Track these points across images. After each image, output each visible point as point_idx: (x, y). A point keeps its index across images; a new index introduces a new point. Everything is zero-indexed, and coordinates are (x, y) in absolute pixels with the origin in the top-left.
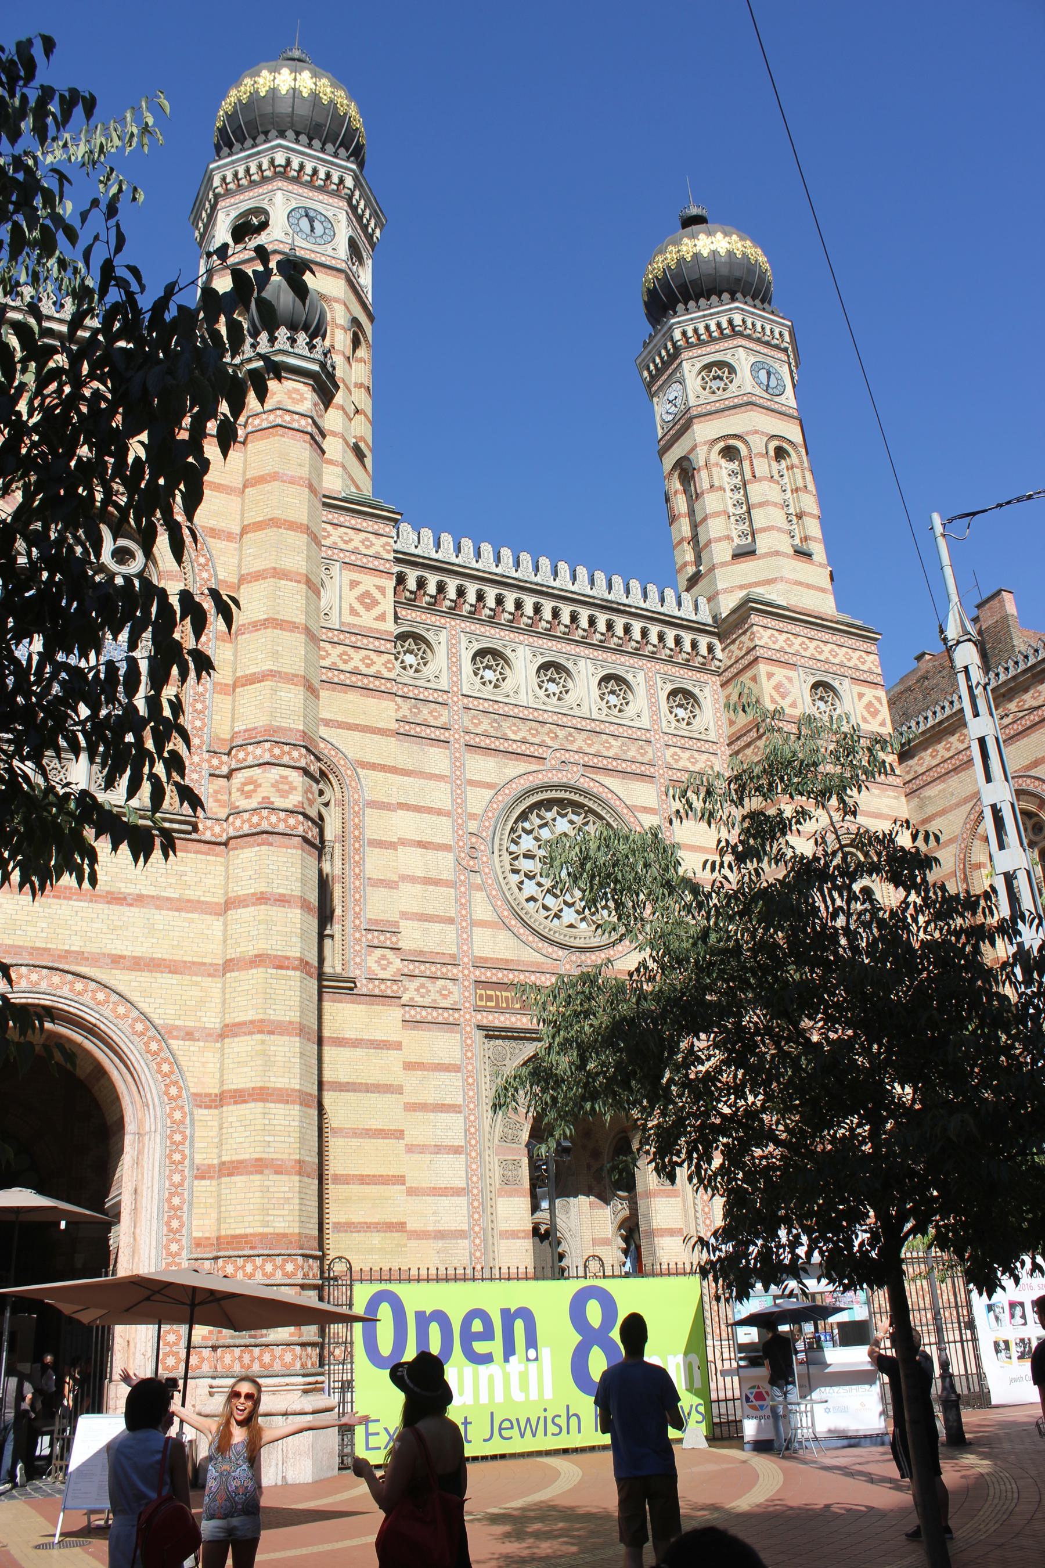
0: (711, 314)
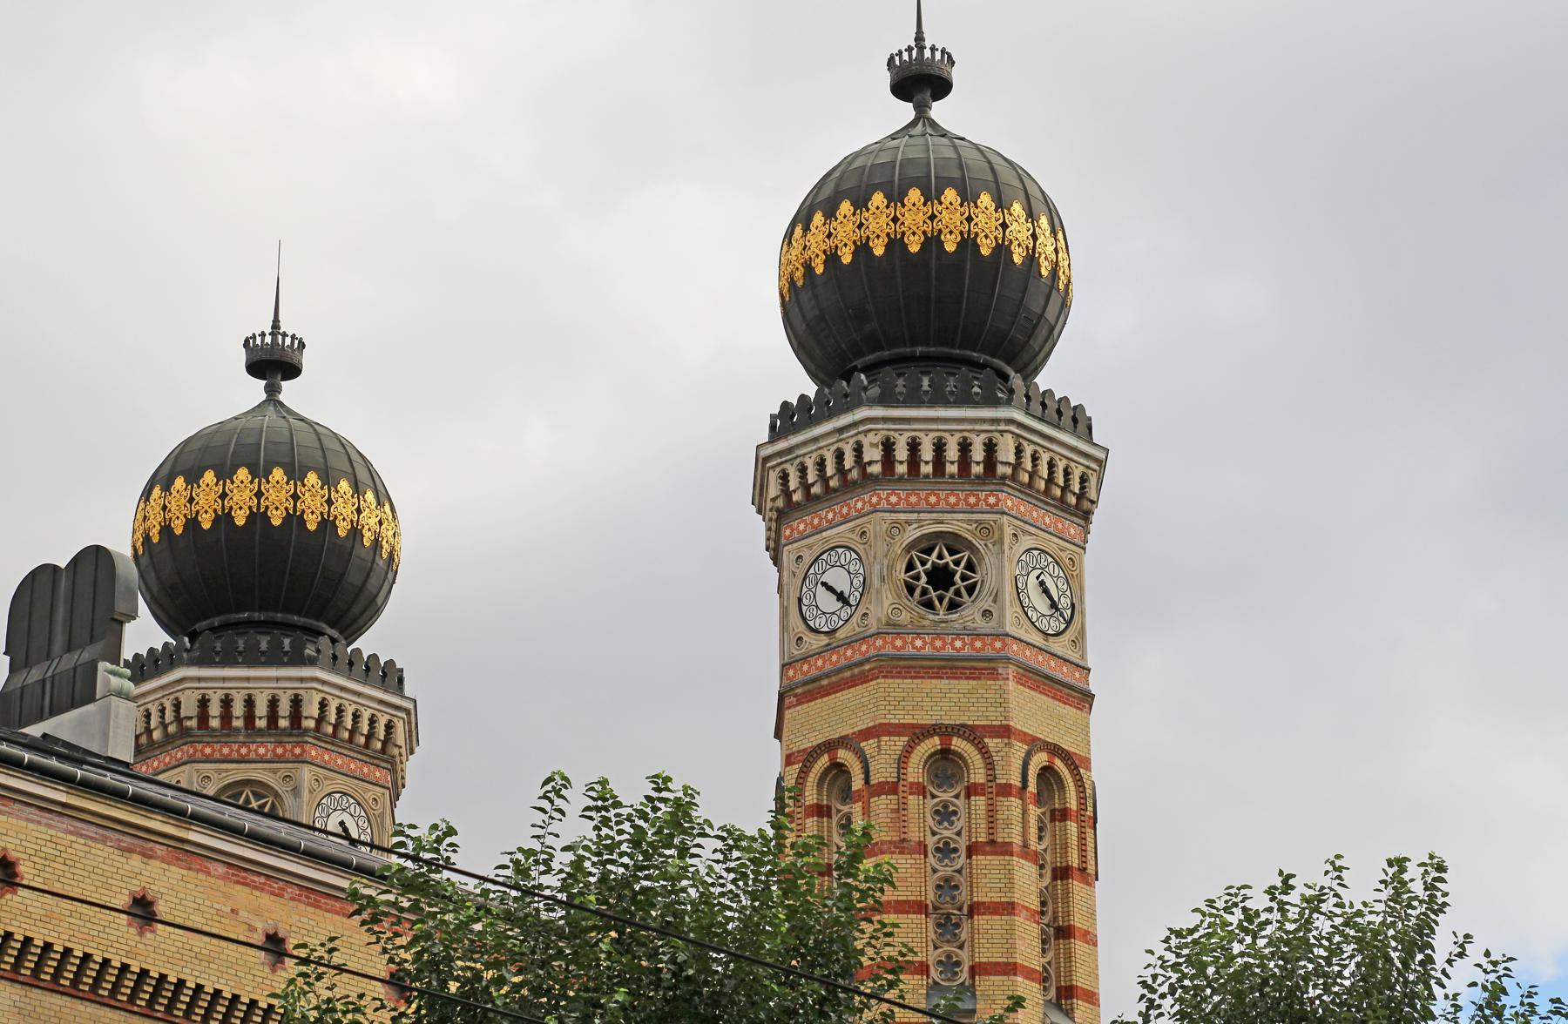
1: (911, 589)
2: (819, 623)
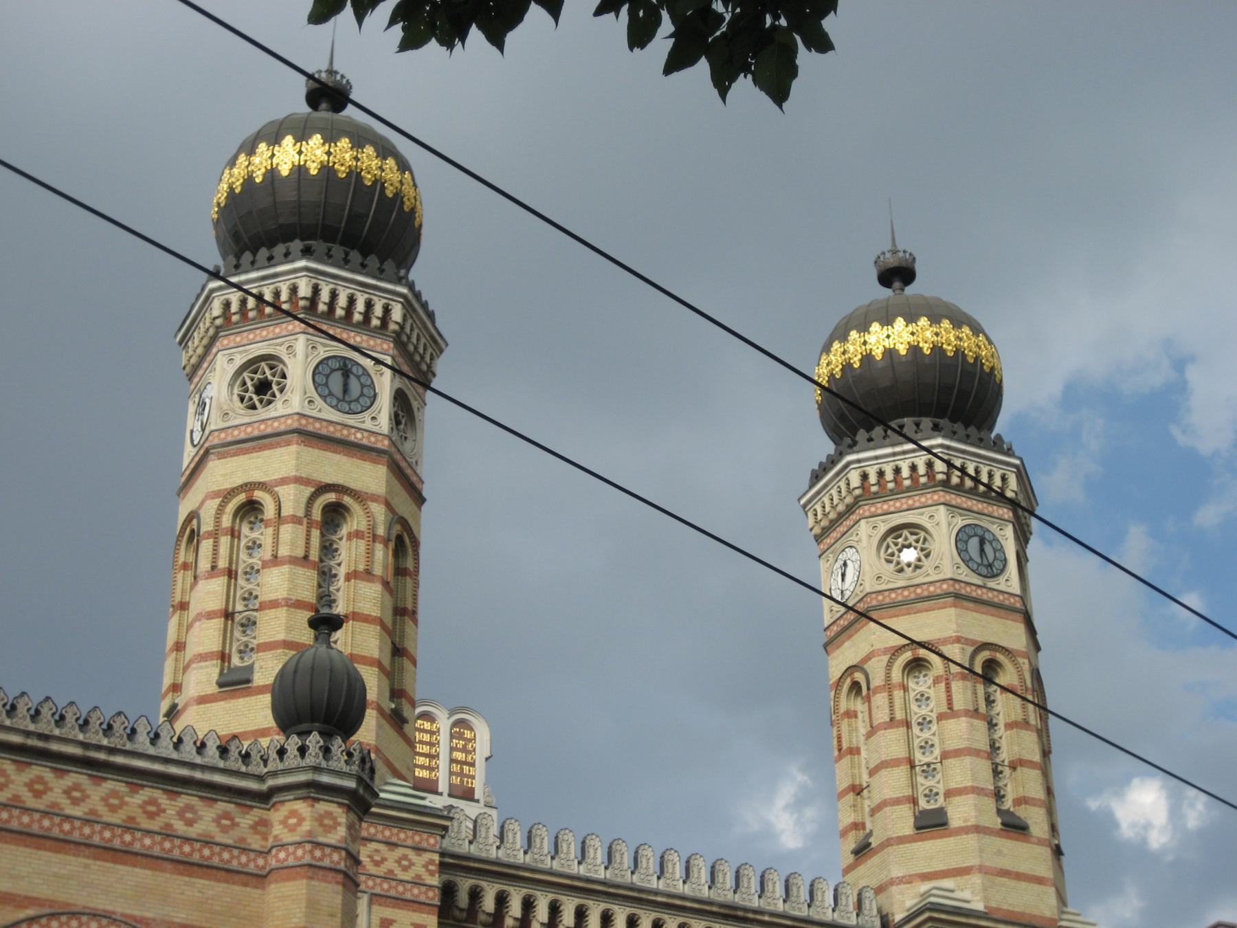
0: (904, 452)
1: (242, 399)
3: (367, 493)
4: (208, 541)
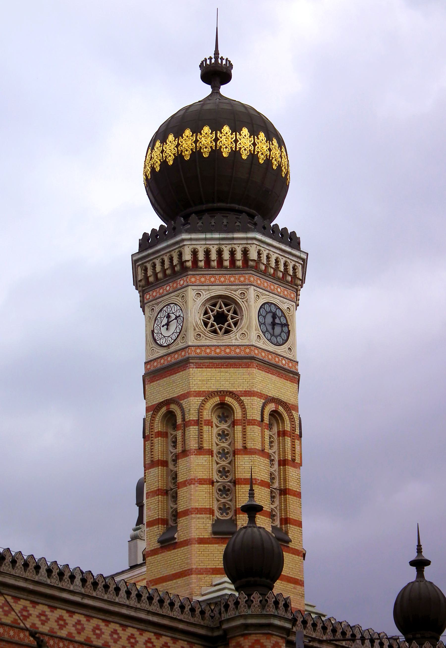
1: (206, 324)
2: (162, 342)
3: (290, 404)
4: (194, 427)
